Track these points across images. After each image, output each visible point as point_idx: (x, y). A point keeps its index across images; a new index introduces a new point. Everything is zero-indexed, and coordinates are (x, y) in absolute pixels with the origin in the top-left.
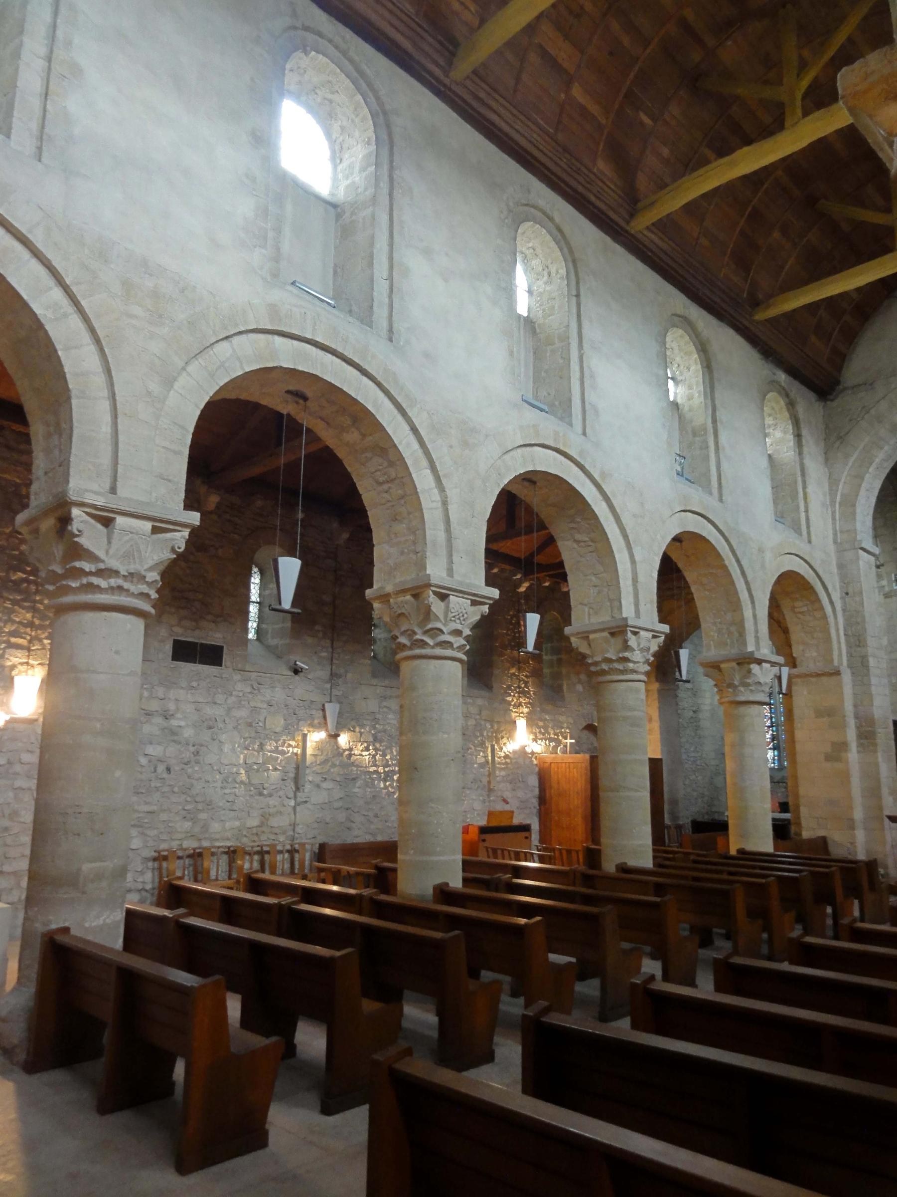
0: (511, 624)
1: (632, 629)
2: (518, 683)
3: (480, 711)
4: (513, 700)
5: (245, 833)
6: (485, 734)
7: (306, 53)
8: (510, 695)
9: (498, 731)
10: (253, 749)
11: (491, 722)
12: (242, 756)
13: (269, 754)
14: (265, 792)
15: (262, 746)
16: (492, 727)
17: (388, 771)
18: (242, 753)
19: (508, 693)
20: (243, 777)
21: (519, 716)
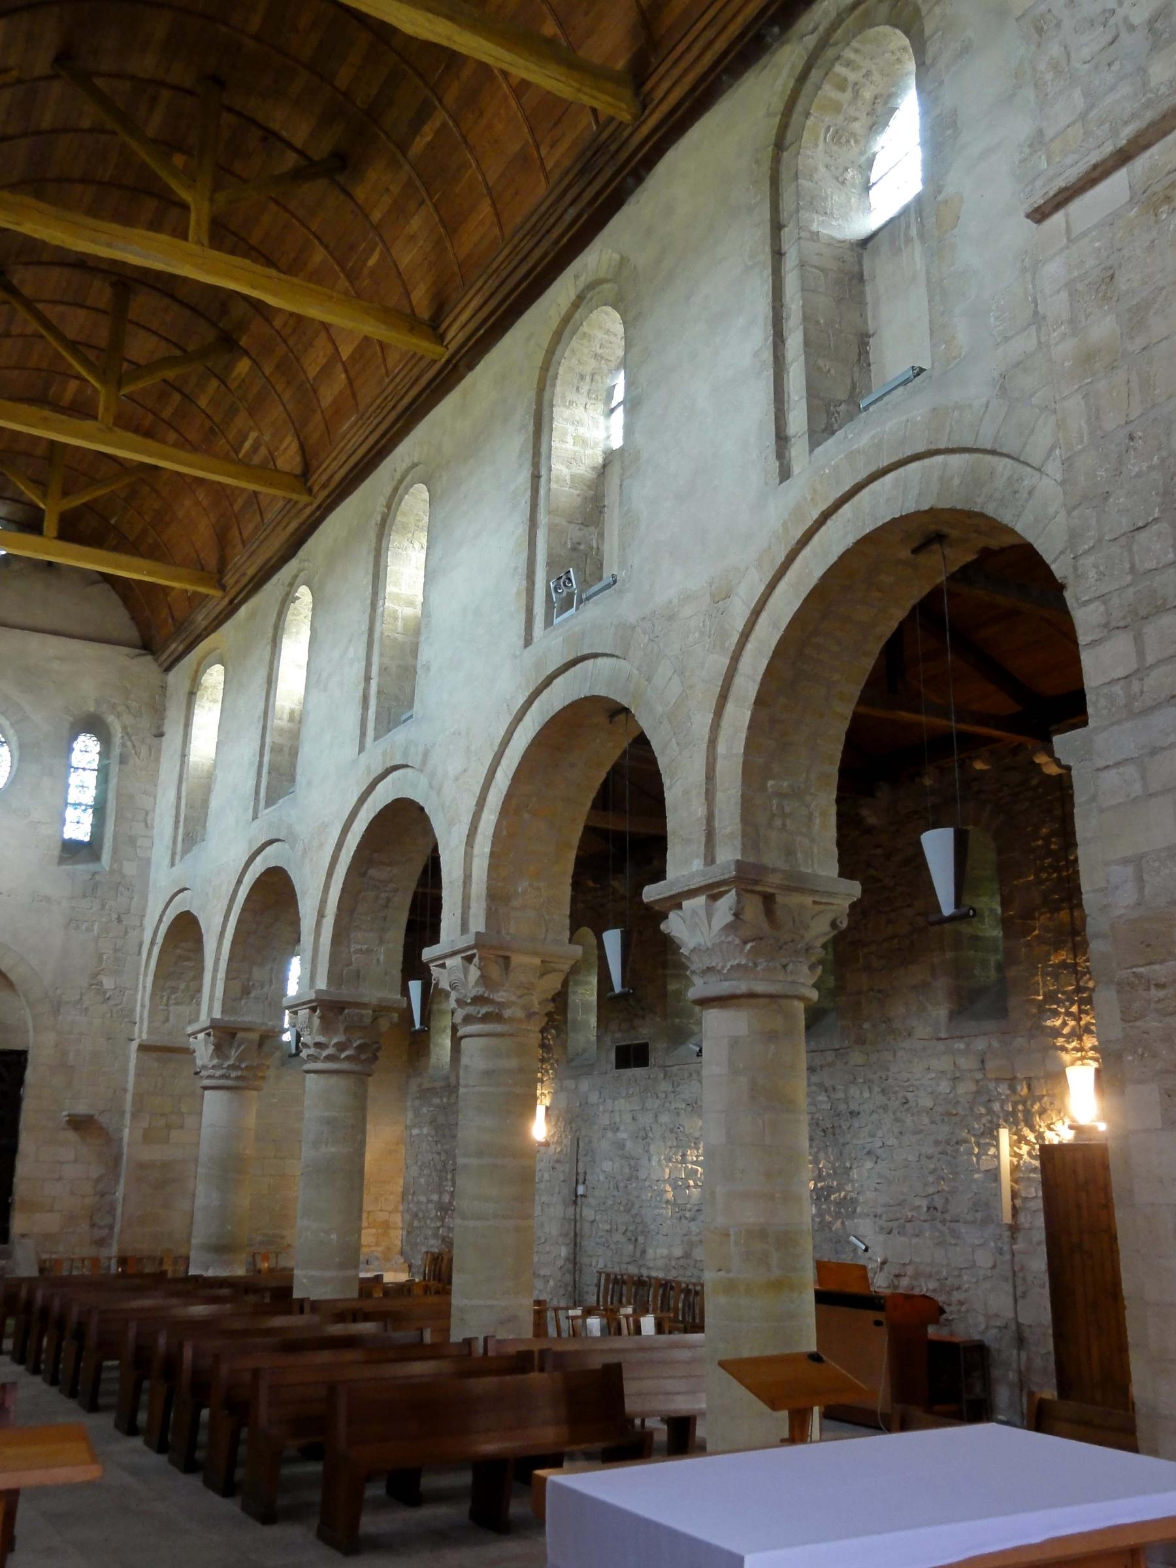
0: (1050, 853)
1: (435, 964)
2: (1075, 983)
3: (983, 1062)
4: (1065, 1024)
5: (673, 1263)
6: (996, 1107)
7: (298, 598)
8: (1056, 1014)
9: (1033, 1097)
10: (677, 1161)
11: (1012, 1083)
12: (667, 1171)
13: (690, 1166)
14: (688, 1215)
15: (684, 1155)
16: (1013, 1089)
17: (822, 1188)
18: (667, 1166)
19: (1050, 1010)
20: (670, 1196)
21: (1082, 1058)
